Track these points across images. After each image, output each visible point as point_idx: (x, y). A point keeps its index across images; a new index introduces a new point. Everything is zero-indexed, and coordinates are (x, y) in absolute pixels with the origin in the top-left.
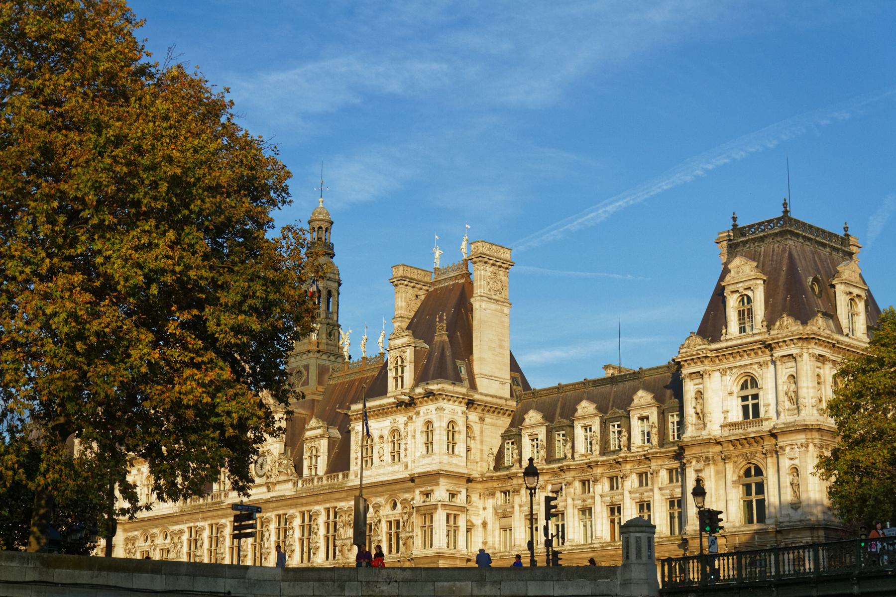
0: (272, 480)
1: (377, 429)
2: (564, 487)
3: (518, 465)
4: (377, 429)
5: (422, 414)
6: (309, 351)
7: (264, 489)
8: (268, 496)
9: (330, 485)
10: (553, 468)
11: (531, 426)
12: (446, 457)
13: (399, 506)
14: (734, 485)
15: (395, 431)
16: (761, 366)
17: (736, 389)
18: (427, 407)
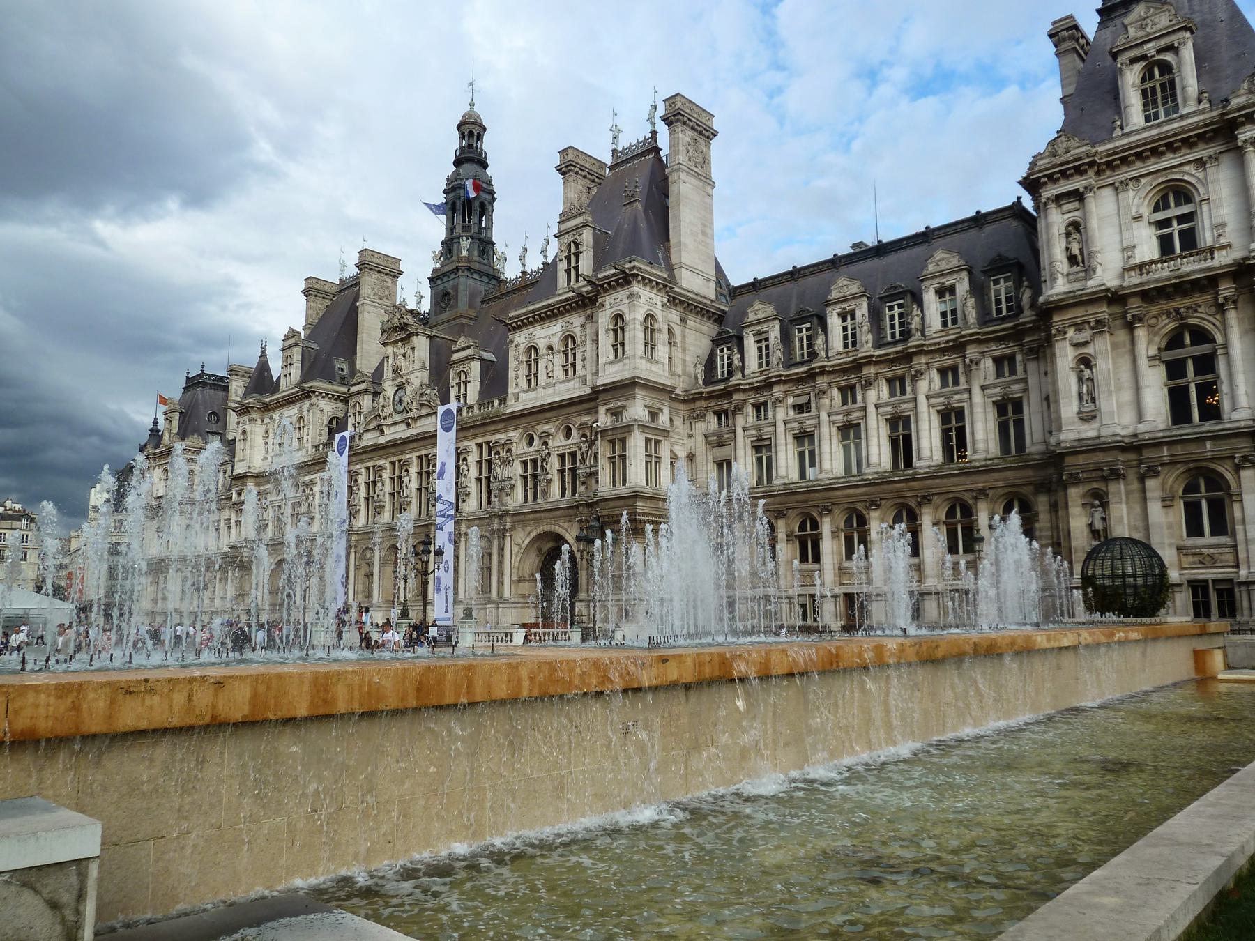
0: (415, 413)
1: (544, 338)
2: (813, 399)
3: (739, 375)
4: (544, 338)
5: (607, 305)
6: (458, 269)
7: (403, 427)
8: (408, 433)
9: (483, 414)
10: (797, 373)
11: (759, 322)
12: (644, 362)
13: (574, 433)
14: (1152, 363)
15: (569, 338)
16: (1205, 163)
17: (1145, 210)
18: (615, 296)
